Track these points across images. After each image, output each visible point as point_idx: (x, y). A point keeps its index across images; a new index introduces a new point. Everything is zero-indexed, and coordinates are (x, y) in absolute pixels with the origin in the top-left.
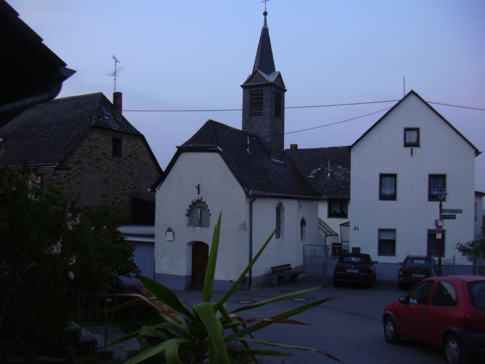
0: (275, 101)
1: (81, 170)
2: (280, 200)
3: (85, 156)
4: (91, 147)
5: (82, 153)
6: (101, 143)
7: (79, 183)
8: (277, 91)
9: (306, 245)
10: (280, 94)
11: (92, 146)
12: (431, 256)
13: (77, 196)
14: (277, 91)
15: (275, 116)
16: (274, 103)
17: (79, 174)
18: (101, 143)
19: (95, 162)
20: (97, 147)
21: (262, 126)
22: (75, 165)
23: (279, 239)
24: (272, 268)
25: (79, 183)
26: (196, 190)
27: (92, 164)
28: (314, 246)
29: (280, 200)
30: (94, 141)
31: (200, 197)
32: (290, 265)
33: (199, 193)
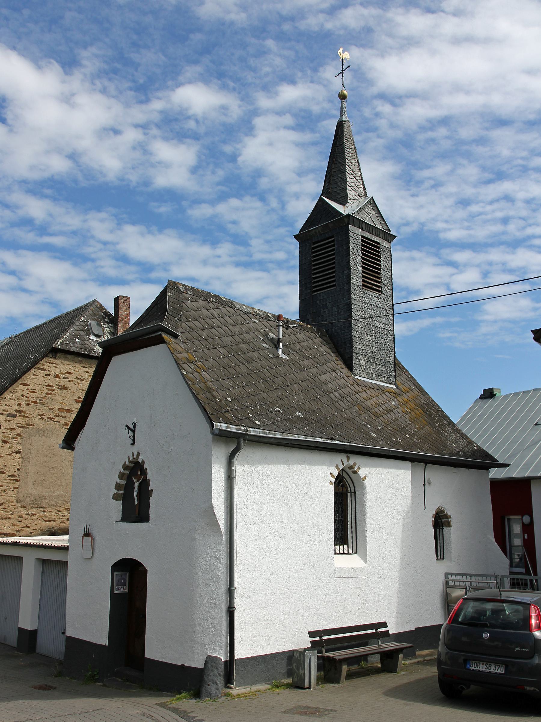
0: (361, 254)
1: (23, 427)
2: (348, 458)
3: (35, 403)
4: (50, 388)
5: (27, 397)
6: (72, 381)
7: (18, 452)
8: (368, 235)
9: (452, 574)
10: (378, 243)
11: (52, 386)
12: (281, 683)
13: (13, 476)
14: (368, 235)
15: (363, 285)
16: (360, 259)
17: (19, 435)
18: (72, 381)
19: (57, 415)
20: (65, 388)
21: (335, 309)
22: (8, 418)
23: (442, 561)
24: (312, 634)
25: (18, 452)
26: (126, 434)
27: (51, 418)
28: (471, 575)
29: (348, 458)
30: (57, 376)
31: (135, 449)
32: (384, 625)
33: (133, 444)
